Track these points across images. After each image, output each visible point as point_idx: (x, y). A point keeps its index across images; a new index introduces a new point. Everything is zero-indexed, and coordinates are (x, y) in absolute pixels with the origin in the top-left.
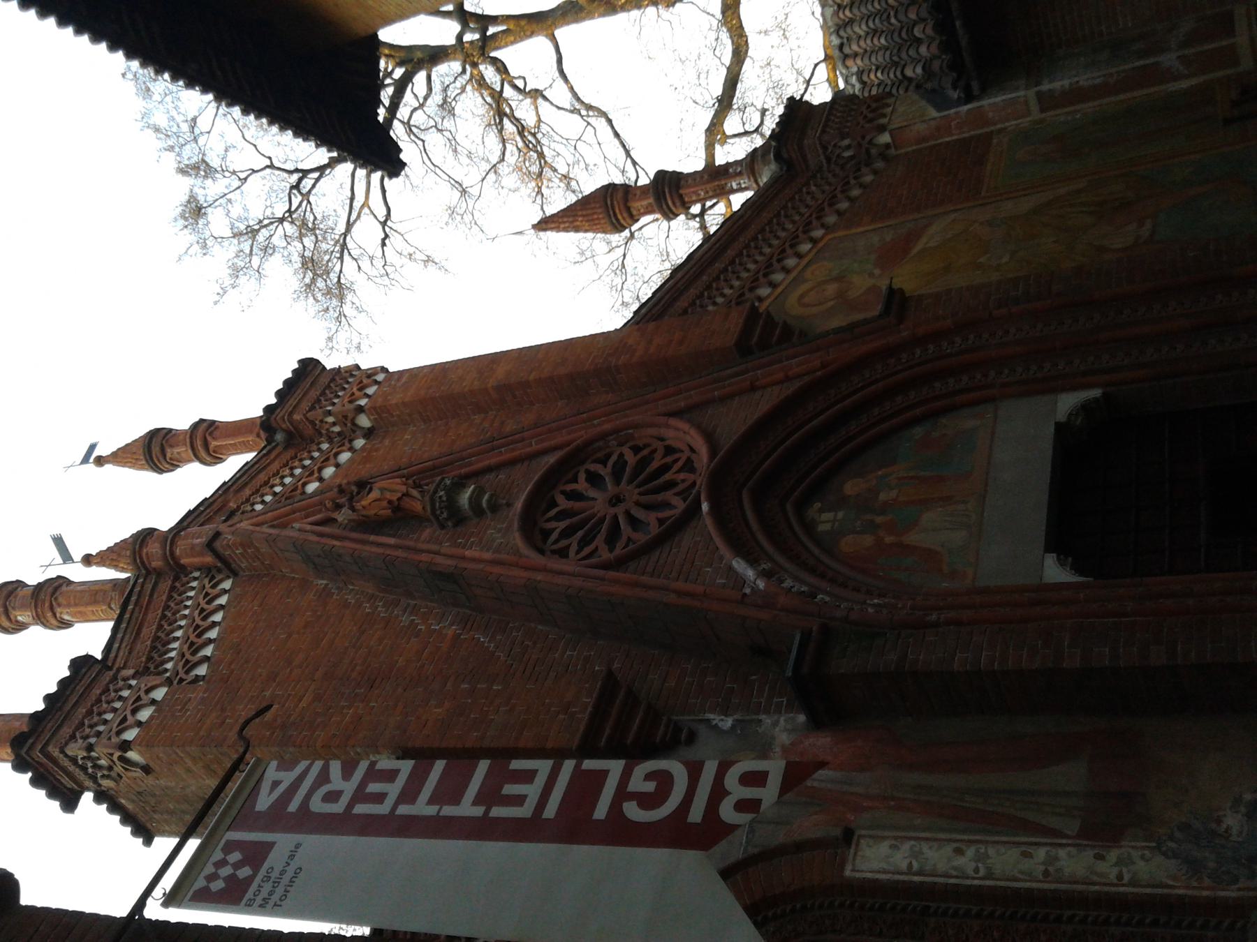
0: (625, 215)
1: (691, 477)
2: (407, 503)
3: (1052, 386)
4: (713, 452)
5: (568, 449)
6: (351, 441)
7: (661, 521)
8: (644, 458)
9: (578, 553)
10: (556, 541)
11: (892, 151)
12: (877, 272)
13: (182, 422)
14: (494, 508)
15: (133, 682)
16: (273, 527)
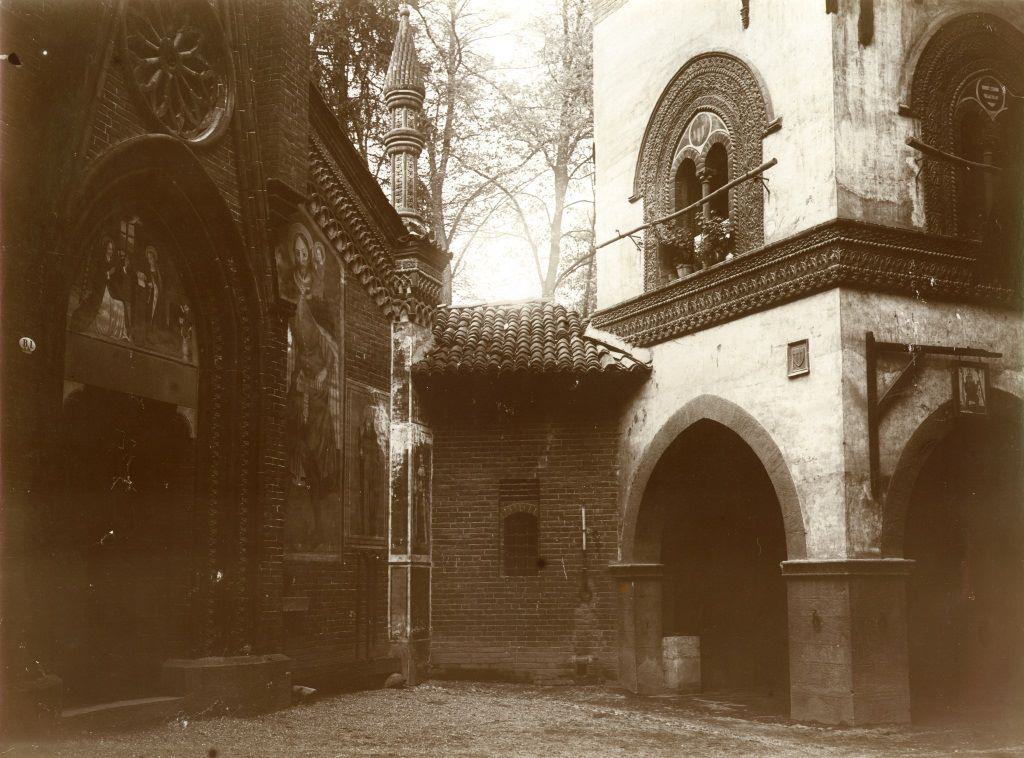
4: (199, 148)
12: (309, 297)
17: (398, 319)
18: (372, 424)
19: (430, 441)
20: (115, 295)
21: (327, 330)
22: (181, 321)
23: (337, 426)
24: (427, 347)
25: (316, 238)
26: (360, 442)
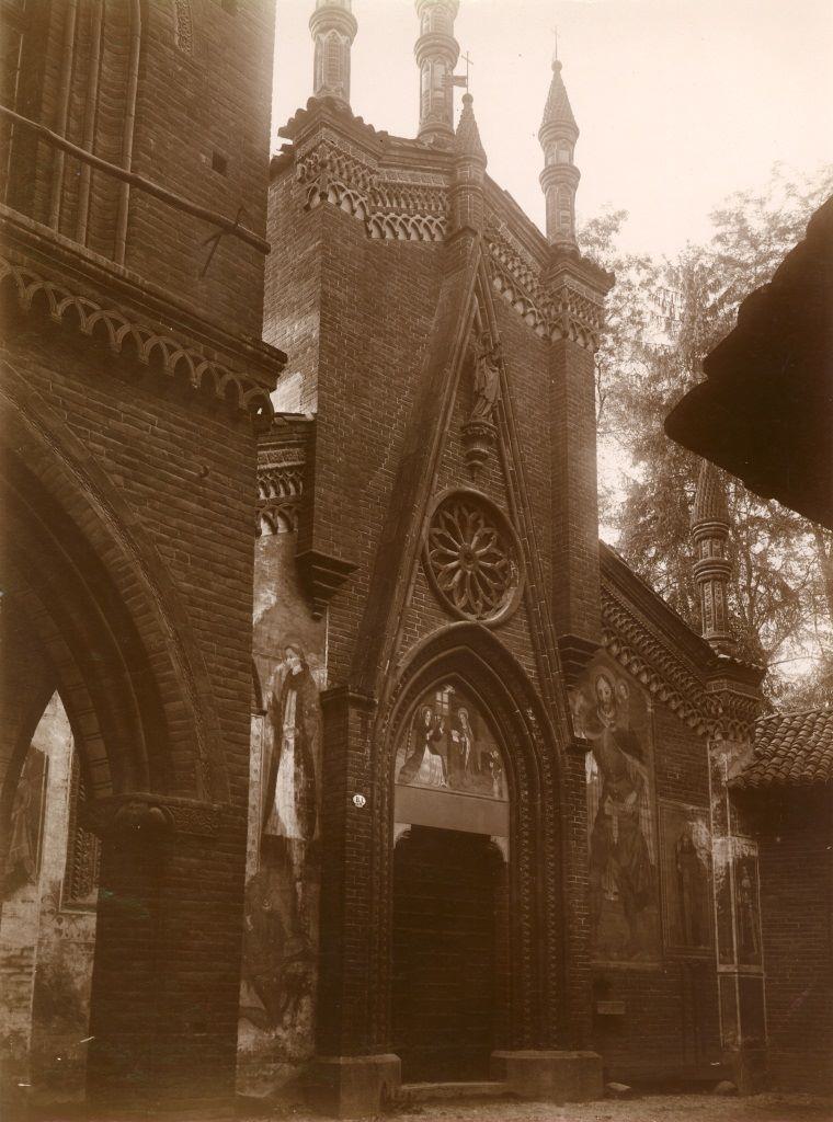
0: (702, 535)
1: (479, 610)
2: (480, 403)
3: (514, 834)
4: (495, 626)
5: (508, 519)
6: (543, 323)
7: (449, 593)
8: (497, 576)
9: (435, 535)
10: (444, 517)
11: (709, 740)
13: (582, 156)
14: (472, 468)
15: (368, 189)
16: (477, 282)
17: (713, 737)
18: (690, 841)
19: (754, 853)
20: (434, 751)
21: (634, 756)
22: (492, 765)
23: (650, 843)
24: (746, 761)
25: (618, 675)
26: (677, 857)
